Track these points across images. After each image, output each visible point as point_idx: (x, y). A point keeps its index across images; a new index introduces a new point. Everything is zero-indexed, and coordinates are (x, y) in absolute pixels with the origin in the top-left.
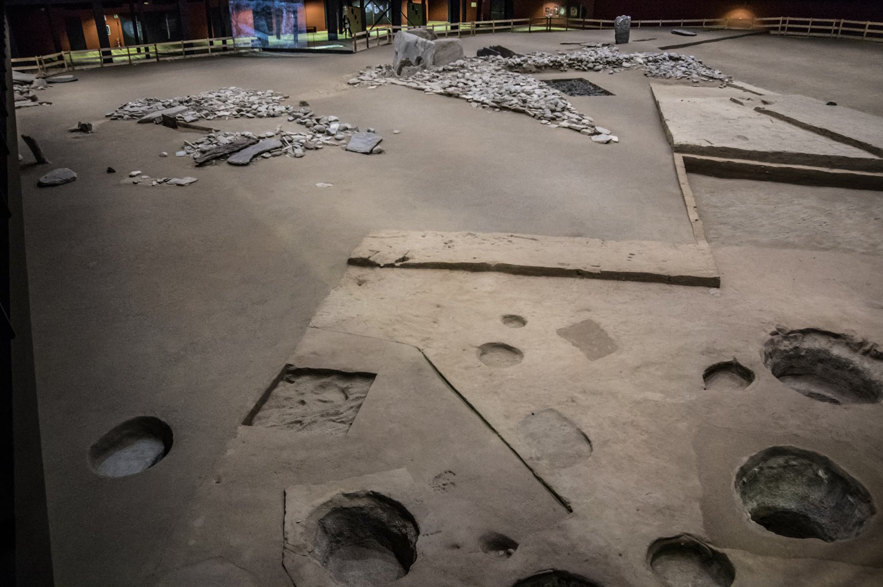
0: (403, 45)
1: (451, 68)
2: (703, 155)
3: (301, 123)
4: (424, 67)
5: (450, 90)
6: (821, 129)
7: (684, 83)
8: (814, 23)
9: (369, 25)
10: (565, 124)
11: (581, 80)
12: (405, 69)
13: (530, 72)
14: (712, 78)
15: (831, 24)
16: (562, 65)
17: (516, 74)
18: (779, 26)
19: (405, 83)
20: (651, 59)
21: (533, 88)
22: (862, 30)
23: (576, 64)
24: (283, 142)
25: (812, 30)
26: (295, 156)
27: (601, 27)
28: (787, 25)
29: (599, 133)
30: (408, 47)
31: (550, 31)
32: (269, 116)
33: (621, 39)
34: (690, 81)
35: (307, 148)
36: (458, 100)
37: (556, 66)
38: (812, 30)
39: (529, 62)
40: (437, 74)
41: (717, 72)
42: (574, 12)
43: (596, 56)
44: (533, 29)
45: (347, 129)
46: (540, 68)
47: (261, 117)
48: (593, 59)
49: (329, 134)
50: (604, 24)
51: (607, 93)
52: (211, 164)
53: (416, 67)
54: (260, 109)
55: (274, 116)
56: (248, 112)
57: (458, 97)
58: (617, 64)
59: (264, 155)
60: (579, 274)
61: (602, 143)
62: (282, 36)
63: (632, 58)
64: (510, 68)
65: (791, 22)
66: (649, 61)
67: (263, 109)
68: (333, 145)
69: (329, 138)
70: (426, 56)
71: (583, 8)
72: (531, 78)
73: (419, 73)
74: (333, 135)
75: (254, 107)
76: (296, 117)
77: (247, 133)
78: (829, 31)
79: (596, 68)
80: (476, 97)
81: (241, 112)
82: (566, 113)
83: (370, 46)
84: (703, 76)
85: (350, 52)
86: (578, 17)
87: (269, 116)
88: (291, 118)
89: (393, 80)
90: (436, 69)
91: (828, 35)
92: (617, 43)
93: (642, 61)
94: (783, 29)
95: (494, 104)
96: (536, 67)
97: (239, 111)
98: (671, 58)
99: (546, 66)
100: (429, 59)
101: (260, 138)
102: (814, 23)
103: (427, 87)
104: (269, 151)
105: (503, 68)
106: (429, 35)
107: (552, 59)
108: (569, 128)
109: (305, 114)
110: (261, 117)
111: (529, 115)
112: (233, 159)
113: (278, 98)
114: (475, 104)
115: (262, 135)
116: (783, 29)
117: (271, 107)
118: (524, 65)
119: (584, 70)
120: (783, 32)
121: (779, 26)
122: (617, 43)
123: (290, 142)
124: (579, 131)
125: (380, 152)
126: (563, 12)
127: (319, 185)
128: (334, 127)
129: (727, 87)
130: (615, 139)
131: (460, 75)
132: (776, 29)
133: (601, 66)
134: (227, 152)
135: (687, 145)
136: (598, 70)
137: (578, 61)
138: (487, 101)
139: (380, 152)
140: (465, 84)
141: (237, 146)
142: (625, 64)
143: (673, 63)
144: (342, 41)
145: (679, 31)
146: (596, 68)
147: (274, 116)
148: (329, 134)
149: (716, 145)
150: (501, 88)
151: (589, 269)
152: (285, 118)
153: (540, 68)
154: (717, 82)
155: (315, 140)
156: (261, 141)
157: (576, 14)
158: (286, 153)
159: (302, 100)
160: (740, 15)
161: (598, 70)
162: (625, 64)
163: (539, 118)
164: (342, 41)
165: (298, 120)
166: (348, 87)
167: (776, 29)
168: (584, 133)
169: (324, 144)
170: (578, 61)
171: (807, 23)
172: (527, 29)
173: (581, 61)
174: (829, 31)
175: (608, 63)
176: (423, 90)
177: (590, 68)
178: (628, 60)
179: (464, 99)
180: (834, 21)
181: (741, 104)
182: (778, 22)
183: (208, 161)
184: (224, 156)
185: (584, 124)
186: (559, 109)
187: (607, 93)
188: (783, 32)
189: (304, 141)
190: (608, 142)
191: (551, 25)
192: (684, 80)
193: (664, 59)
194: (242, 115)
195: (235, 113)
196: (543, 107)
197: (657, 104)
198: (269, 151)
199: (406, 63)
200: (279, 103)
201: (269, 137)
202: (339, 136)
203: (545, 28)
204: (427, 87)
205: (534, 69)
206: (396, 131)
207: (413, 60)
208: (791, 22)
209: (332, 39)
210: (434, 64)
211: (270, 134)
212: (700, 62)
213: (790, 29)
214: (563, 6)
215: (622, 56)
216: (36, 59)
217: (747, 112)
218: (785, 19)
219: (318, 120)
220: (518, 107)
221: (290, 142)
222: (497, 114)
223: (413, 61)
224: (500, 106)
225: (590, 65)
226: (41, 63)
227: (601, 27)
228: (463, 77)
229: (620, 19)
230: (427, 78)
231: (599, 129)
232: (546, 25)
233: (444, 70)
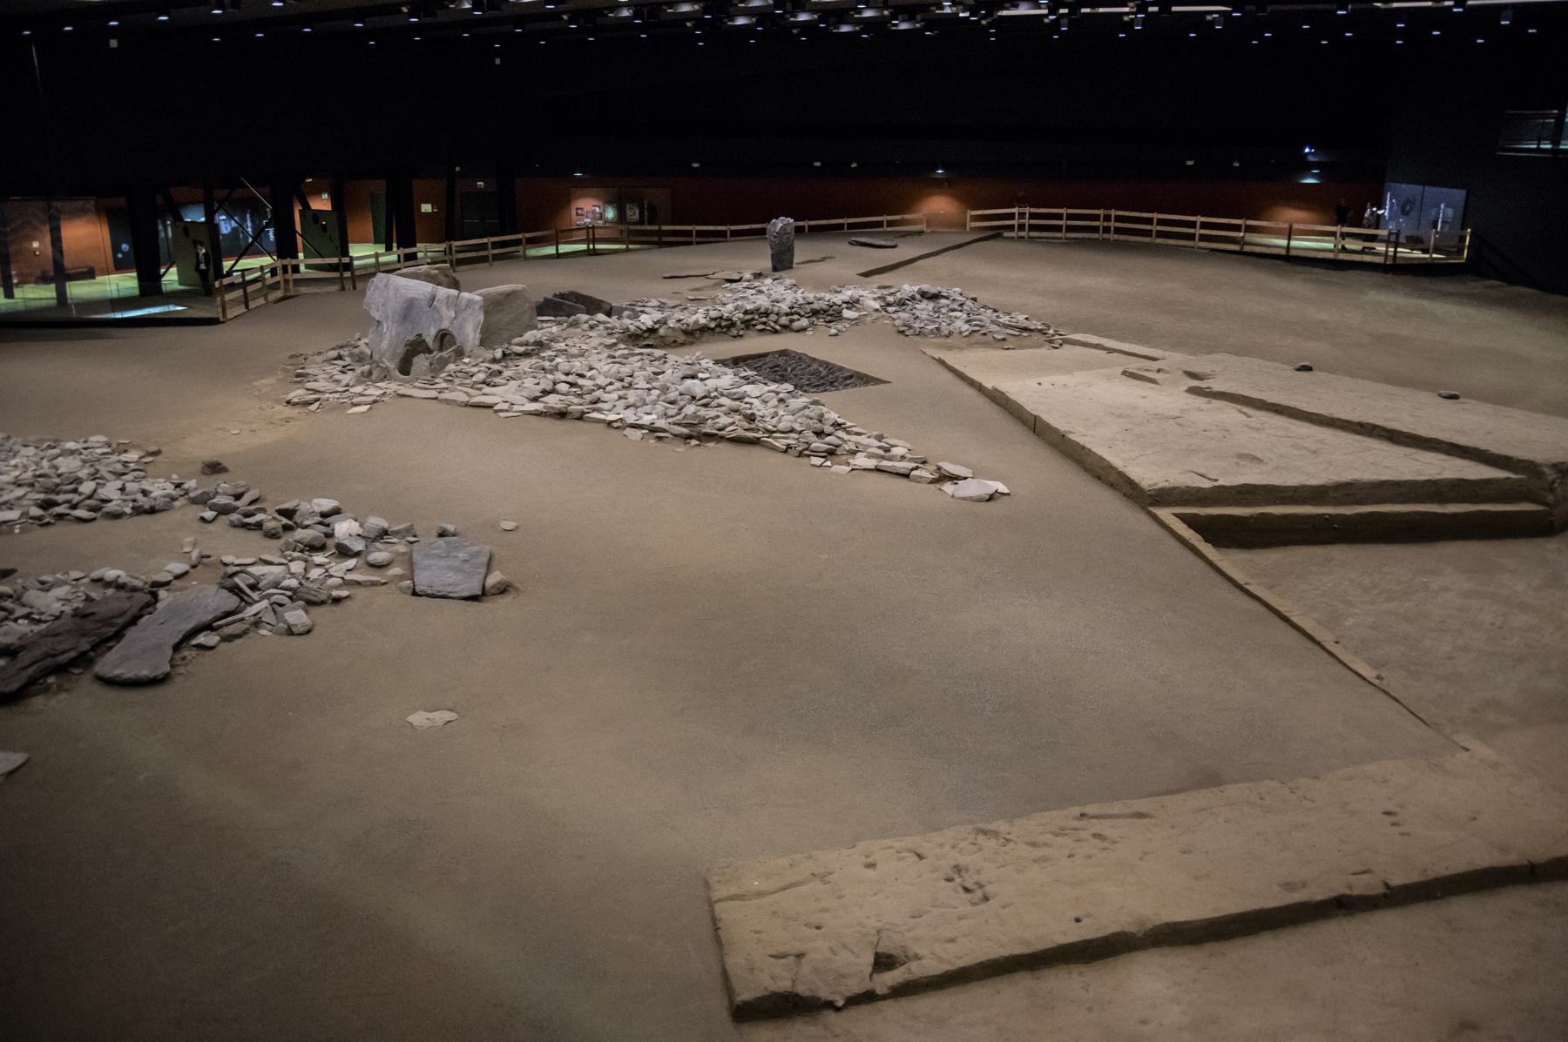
0: (395, 305)
1: (521, 349)
2: (1205, 505)
3: (245, 526)
4: (460, 353)
5: (553, 401)
6: (1361, 425)
7: (986, 345)
8: (1070, 217)
9: (229, 256)
10: (861, 461)
11: (783, 353)
12: (421, 362)
13: (675, 344)
14: (1026, 329)
15: (1096, 218)
16: (733, 324)
17: (658, 353)
19: (434, 394)
20: (890, 299)
21: (712, 377)
23: (754, 321)
24: (235, 590)
25: (1070, 229)
26: (290, 632)
27: (694, 239)
29: (954, 478)
30: (409, 310)
31: (595, 253)
32: (138, 511)
33: (782, 262)
34: (989, 338)
35: (310, 603)
36: (579, 424)
37: (724, 327)
38: (1070, 229)
39: (671, 324)
40: (495, 367)
41: (1021, 318)
42: (633, 213)
43: (788, 302)
44: (564, 248)
45: (385, 532)
46: (694, 335)
47: (116, 516)
48: (785, 307)
49: (344, 552)
50: (700, 234)
51: (878, 381)
52: (46, 690)
53: (444, 354)
54: (104, 493)
55: (152, 511)
56: (74, 507)
57: (581, 417)
58: (831, 314)
59: (201, 639)
60: (1343, 906)
61: (980, 500)
62: (18, 292)
63: (857, 301)
64: (636, 338)
65: (1032, 216)
66: (889, 305)
67: (110, 490)
68: (373, 584)
69: (351, 563)
70: (461, 327)
71: (650, 205)
72: (703, 355)
73: (451, 367)
74: (357, 554)
75: (87, 487)
76: (224, 511)
77: (111, 574)
78: (1095, 229)
79: (796, 325)
80: (630, 416)
81: (54, 504)
82: (840, 433)
83: (252, 305)
84: (1006, 326)
85: (213, 322)
86: (641, 222)
87: (138, 511)
88: (209, 514)
89: (393, 387)
90: (489, 355)
92: (775, 269)
93: (877, 305)
95: (685, 431)
96: (686, 332)
97: (46, 505)
98: (924, 295)
99: (704, 329)
100: (470, 333)
101: (159, 584)
102: (1070, 217)
103: (494, 396)
104: (208, 627)
105: (620, 340)
106: (442, 278)
107: (713, 314)
108: (878, 470)
109: (238, 497)
110: (116, 516)
111: (773, 448)
112: (112, 663)
113: (132, 456)
114: (639, 433)
115: (162, 577)
116: (1021, 227)
117: (130, 487)
118: (662, 331)
119: (776, 332)
122: (775, 269)
123: (253, 587)
124: (907, 476)
125: (503, 589)
126: (610, 214)
127: (418, 719)
128: (344, 528)
129: (1066, 346)
130: (1002, 488)
131: (547, 364)
132: (1011, 228)
133: (804, 322)
134: (85, 645)
135: (1174, 488)
136: (803, 330)
137: (761, 315)
138: (661, 423)
139: (503, 589)
140: (572, 385)
141: (107, 621)
142: (847, 314)
143: (931, 305)
144: (174, 297)
145: (863, 240)
146: (796, 325)
147: (152, 511)
148: (344, 552)
149: (1224, 481)
150: (665, 389)
151: (1362, 886)
152: (187, 514)
153: (694, 335)
154: (1036, 337)
155: (315, 573)
156: (162, 593)
157: (637, 216)
158: (257, 623)
159: (208, 456)
160: (939, 205)
161: (803, 330)
162: (847, 314)
163: (801, 454)
164: (174, 297)
165: (235, 517)
166: (295, 412)
167: (1011, 228)
168: (918, 480)
169: (347, 583)
170: (761, 315)
171: (1059, 217)
172: (551, 250)
173: (767, 314)
174: (1095, 229)
175: (815, 313)
176: (490, 407)
177: (784, 327)
178: (852, 304)
179: (603, 421)
180: (1101, 212)
181: (1153, 381)
182: (1011, 216)
183: (32, 681)
184: (84, 660)
185: (903, 457)
186: (828, 429)
187: (866, 380)
188: (1022, 234)
189: (293, 583)
190: (991, 498)
191: (594, 241)
192: (977, 336)
193: (913, 298)
194: (60, 517)
195: (39, 512)
196: (797, 427)
197: (999, 399)
198: (208, 627)
199: (417, 347)
200: (142, 470)
201: (178, 577)
202: (378, 556)
203: (583, 247)
204: (494, 396)
205: (682, 338)
206: (509, 525)
207: (430, 337)
208: (1032, 216)
209: (150, 289)
210: (482, 343)
211: (179, 568)
212: (974, 299)
213: (1033, 228)
214: (609, 202)
215: (838, 299)
217: (1170, 398)
219: (288, 513)
220: (741, 432)
221: (253, 587)
222: (697, 450)
223: (429, 340)
224: (696, 434)
225: (784, 320)
227: (694, 239)
228: (556, 368)
229: (779, 223)
230: (481, 376)
231: (950, 468)
232: (587, 241)
233: (504, 354)
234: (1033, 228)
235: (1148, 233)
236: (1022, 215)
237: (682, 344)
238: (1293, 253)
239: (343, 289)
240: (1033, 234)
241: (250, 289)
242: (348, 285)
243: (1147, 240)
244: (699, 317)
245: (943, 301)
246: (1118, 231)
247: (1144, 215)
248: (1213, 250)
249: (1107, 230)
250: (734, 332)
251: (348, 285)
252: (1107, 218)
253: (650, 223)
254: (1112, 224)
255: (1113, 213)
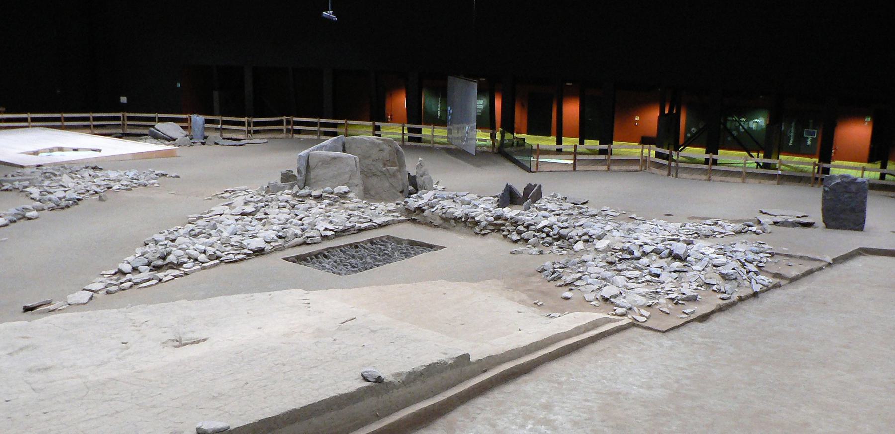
16: (477, 223)
99: (457, 220)
118: (426, 213)
142: (579, 246)
173: (515, 223)
175: (561, 237)
193: (657, 252)
205: (438, 222)
216: (244, 119)
226: (249, 125)
237: (436, 227)
239: (669, 175)
241: (579, 157)
242: (673, 173)
244: (459, 211)
250: (477, 229)
251: (673, 173)
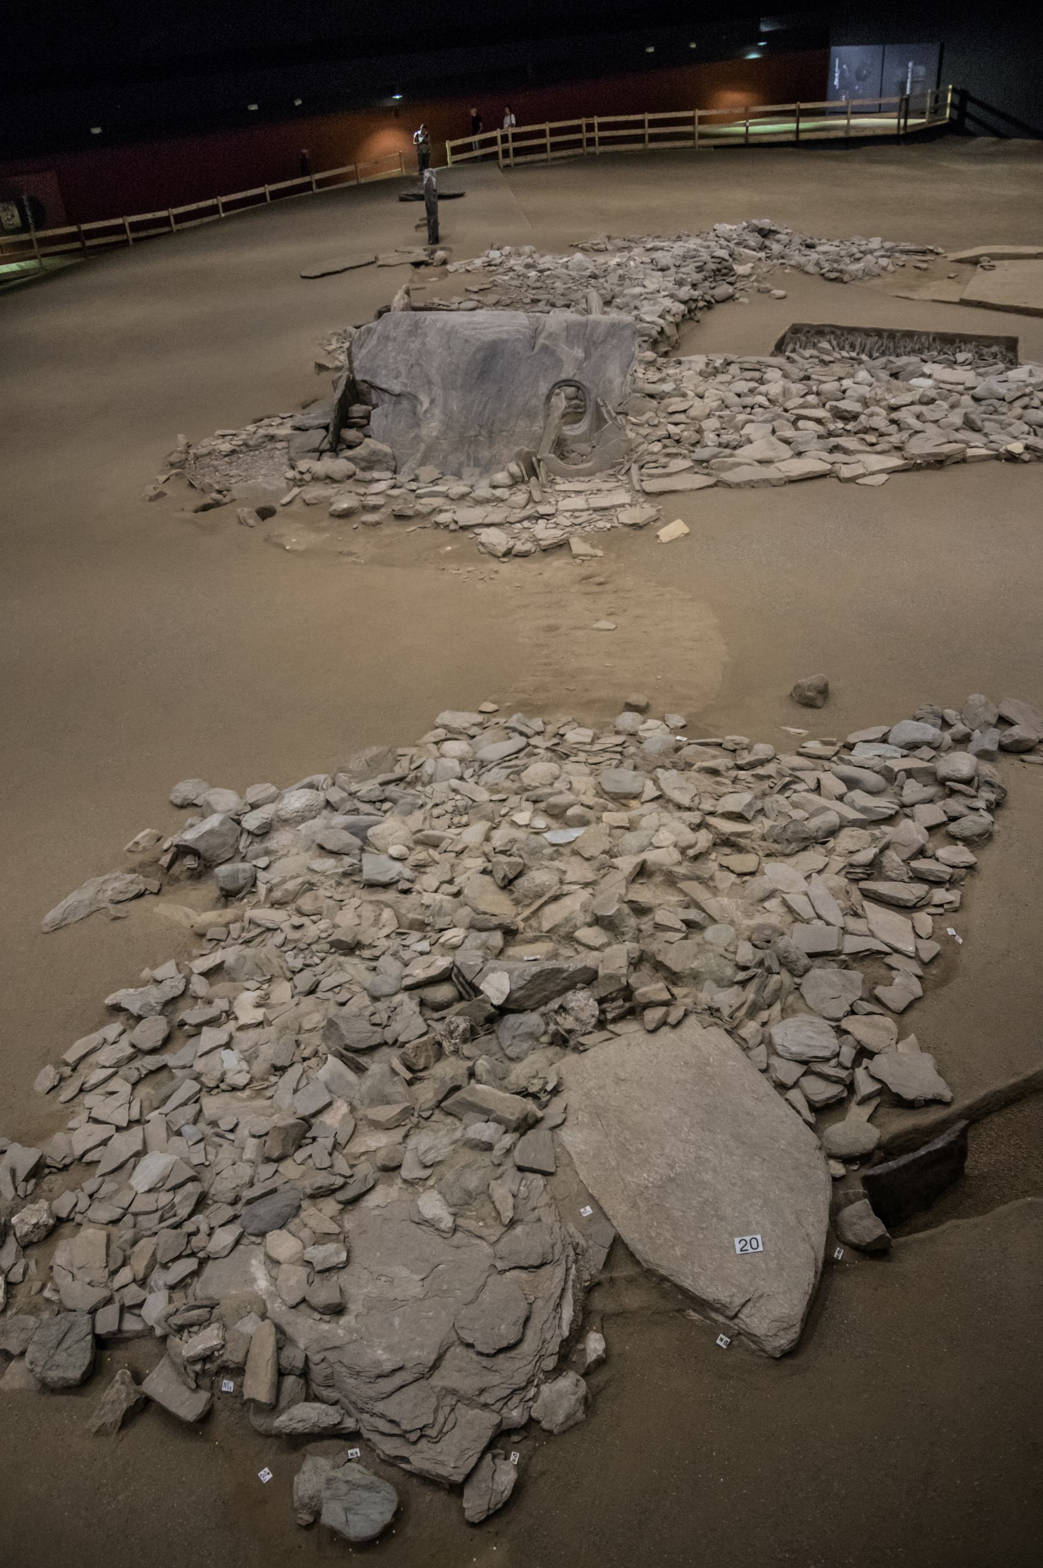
8: (554, 132)
15: (577, 129)
18: (498, 148)
22: (639, 131)
25: (555, 146)
28: (511, 145)
38: (555, 146)
71: (32, 200)
78: (578, 143)
86: (24, 228)
91: (579, 151)
94: (506, 153)
118: (668, 331)
120: (507, 161)
121: (498, 148)
142: (740, 269)
157: (17, 220)
171: (541, 134)
174: (578, 143)
180: (582, 121)
213: (518, 152)
218: (590, 120)
234: (518, 152)
235: (639, 139)
236: (505, 139)
238: (752, 140)
240: (521, 159)
243: (638, 146)
245: (778, 236)
246: (604, 141)
247: (632, 118)
248: (716, 147)
249: (591, 142)
252: (590, 128)
253: (39, 227)
254: (597, 134)
255: (597, 120)
